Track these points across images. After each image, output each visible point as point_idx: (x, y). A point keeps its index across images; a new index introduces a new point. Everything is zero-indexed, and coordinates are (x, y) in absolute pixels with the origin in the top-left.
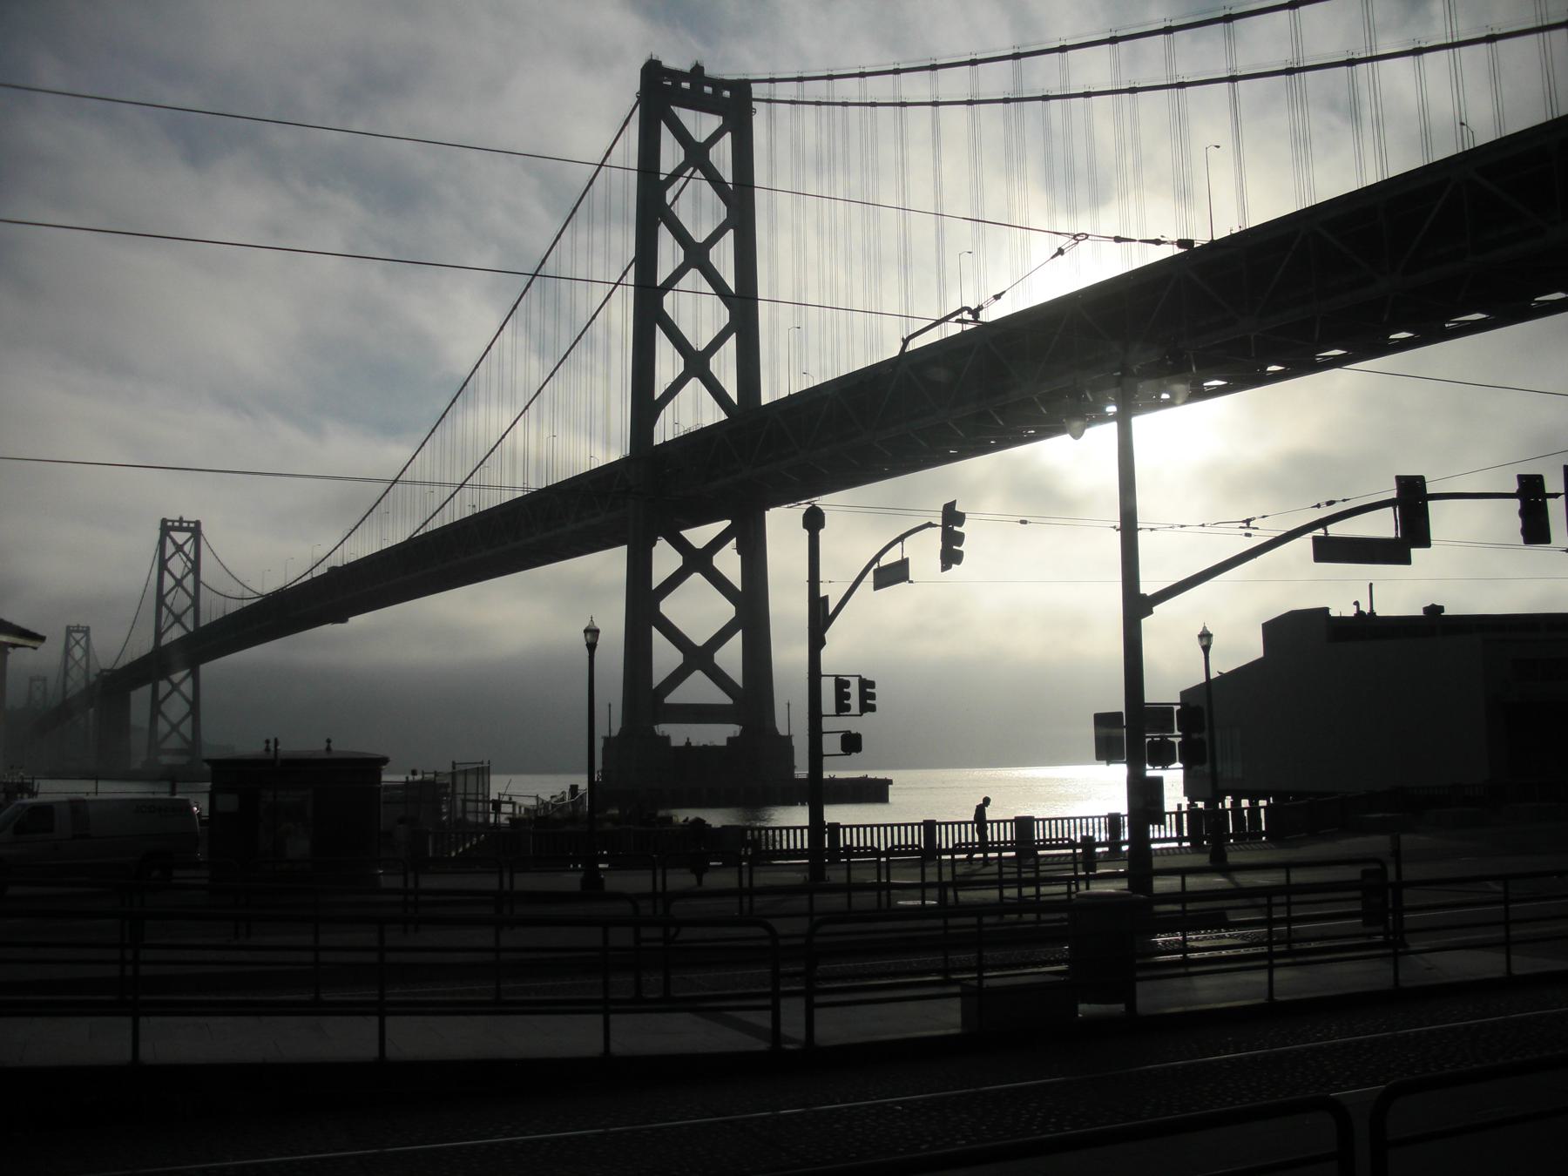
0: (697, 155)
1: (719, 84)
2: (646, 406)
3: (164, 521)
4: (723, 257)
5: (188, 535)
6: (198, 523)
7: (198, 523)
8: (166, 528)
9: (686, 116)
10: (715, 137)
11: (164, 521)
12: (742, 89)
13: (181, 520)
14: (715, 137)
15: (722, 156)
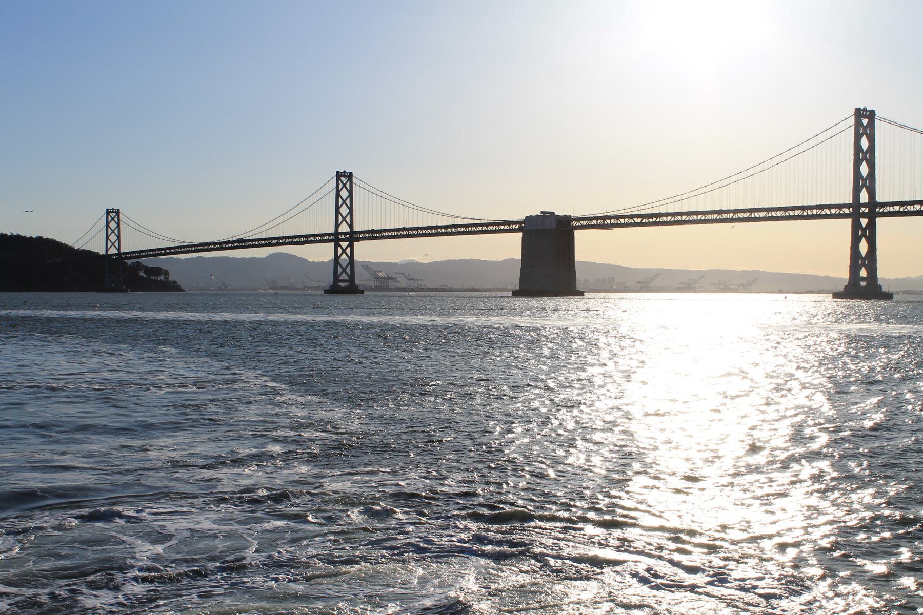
0: (344, 185)
1: (347, 173)
2: (337, 225)
3: (107, 210)
4: (348, 202)
5: (114, 214)
6: (118, 210)
7: (118, 210)
8: (108, 212)
9: (342, 179)
10: (347, 182)
11: (107, 210)
12: (351, 173)
13: (113, 209)
14: (347, 182)
15: (348, 185)
